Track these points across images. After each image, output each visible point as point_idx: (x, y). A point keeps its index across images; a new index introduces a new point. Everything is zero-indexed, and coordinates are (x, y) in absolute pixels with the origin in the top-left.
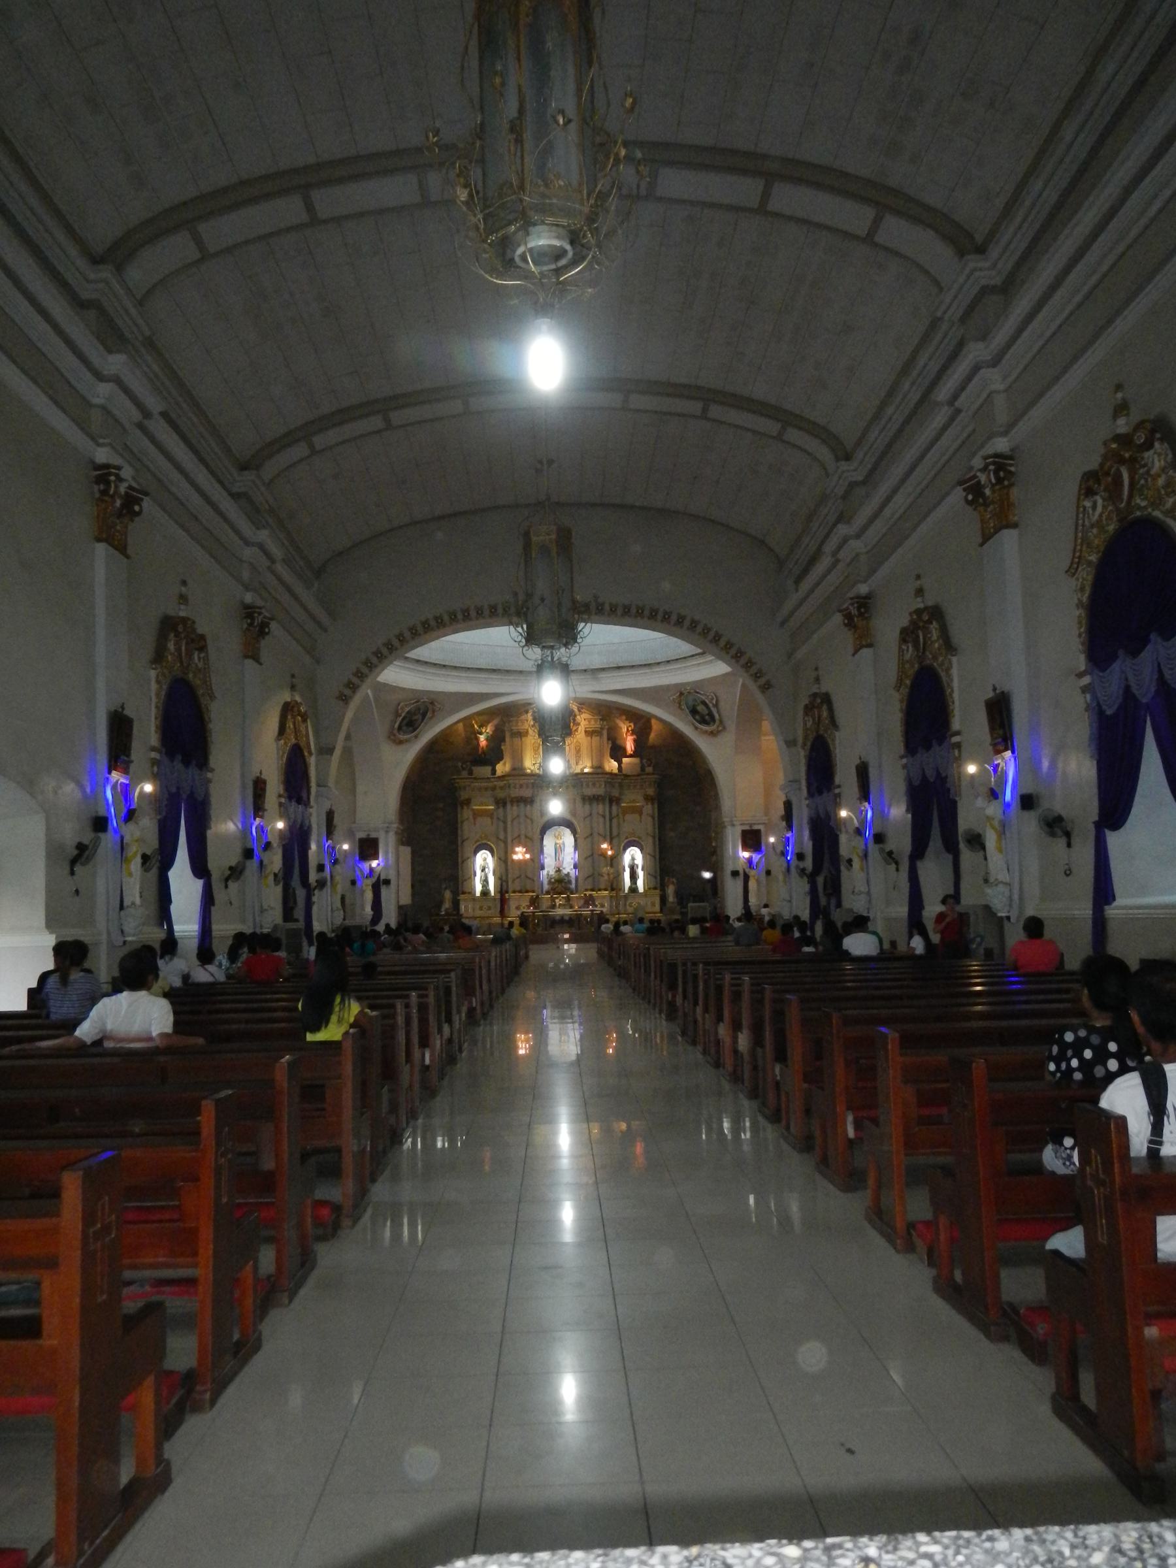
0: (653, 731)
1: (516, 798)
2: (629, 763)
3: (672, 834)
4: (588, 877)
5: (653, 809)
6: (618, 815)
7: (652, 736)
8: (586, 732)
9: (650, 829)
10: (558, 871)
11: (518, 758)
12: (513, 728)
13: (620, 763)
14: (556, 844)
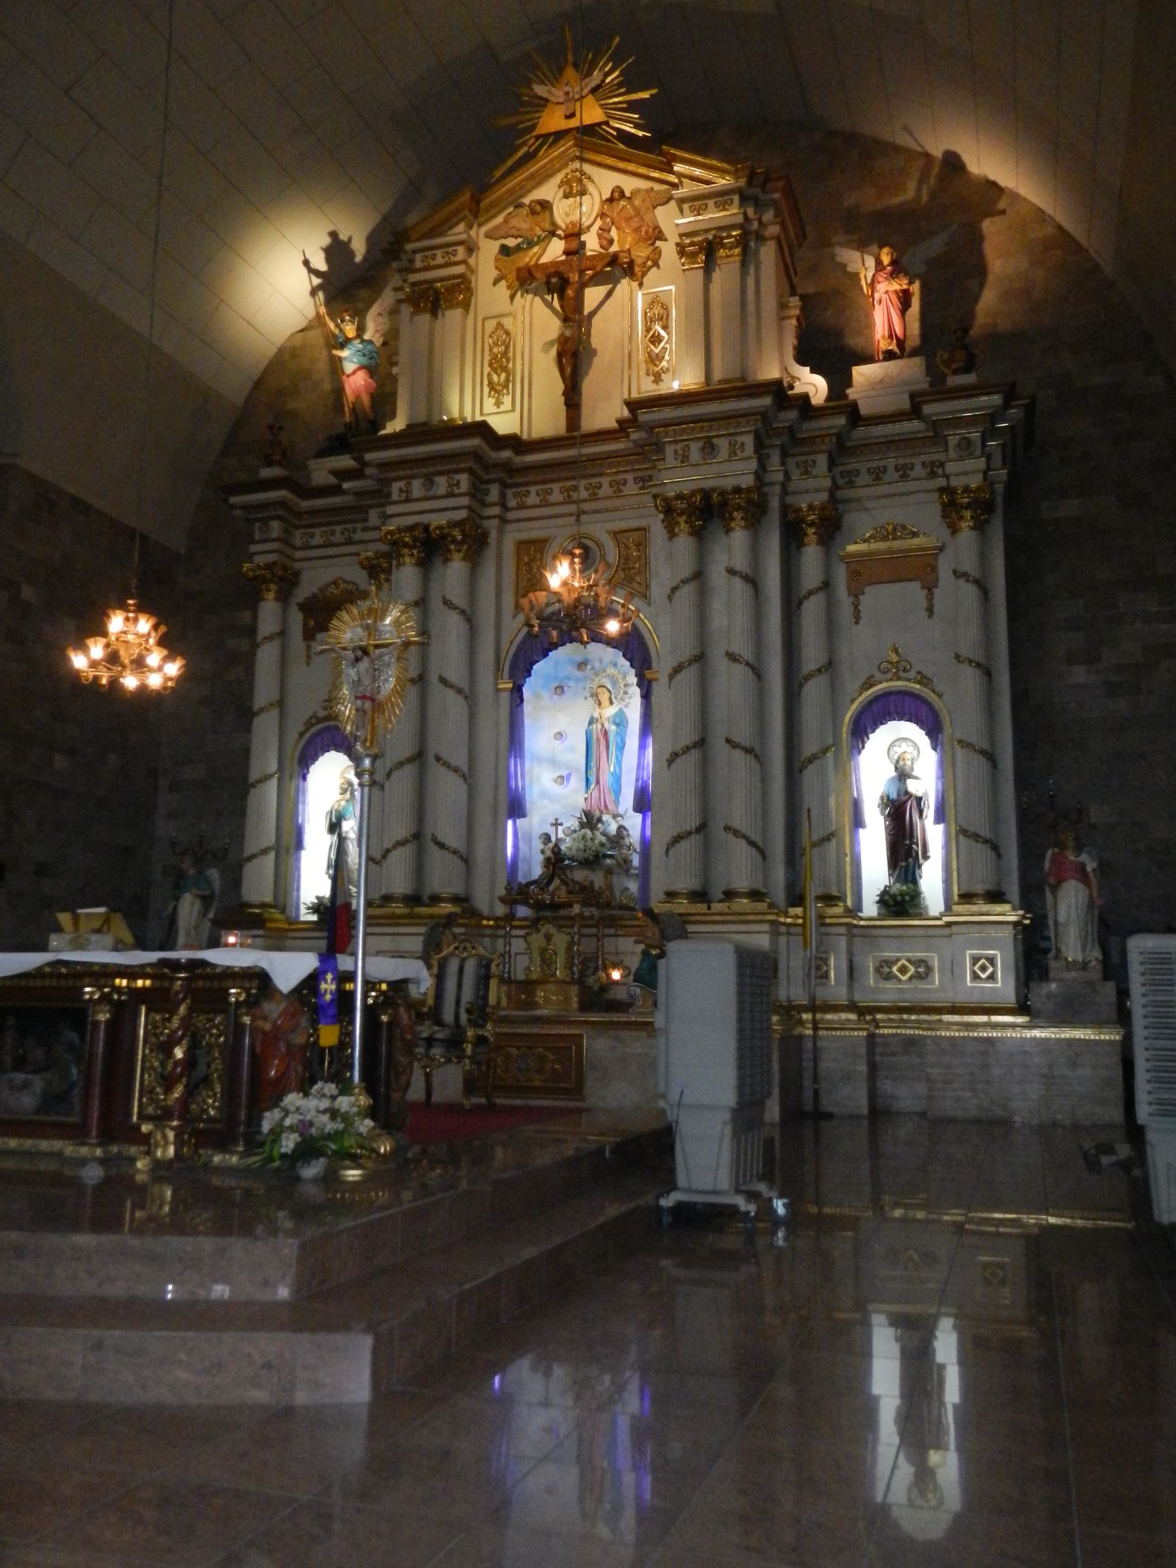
0: (991, 278)
1: (410, 529)
2: (880, 385)
3: (1080, 674)
4: (677, 840)
5: (983, 559)
6: (826, 585)
7: (989, 300)
8: (681, 250)
9: (969, 640)
10: (590, 821)
11: (433, 392)
12: (414, 278)
13: (839, 381)
14: (592, 721)
